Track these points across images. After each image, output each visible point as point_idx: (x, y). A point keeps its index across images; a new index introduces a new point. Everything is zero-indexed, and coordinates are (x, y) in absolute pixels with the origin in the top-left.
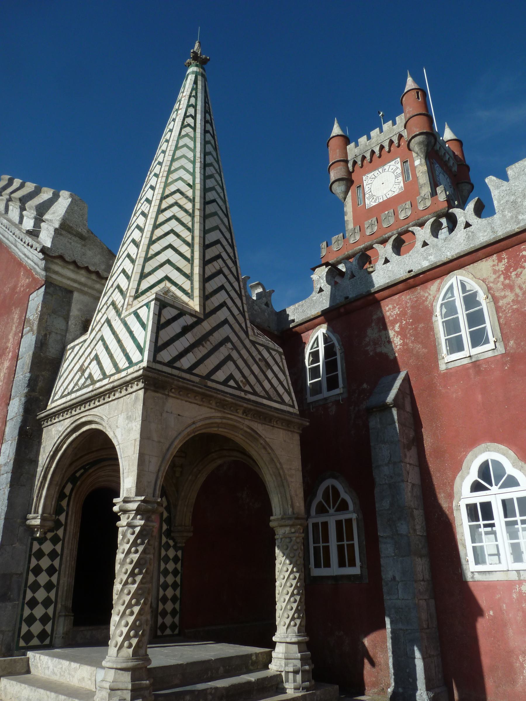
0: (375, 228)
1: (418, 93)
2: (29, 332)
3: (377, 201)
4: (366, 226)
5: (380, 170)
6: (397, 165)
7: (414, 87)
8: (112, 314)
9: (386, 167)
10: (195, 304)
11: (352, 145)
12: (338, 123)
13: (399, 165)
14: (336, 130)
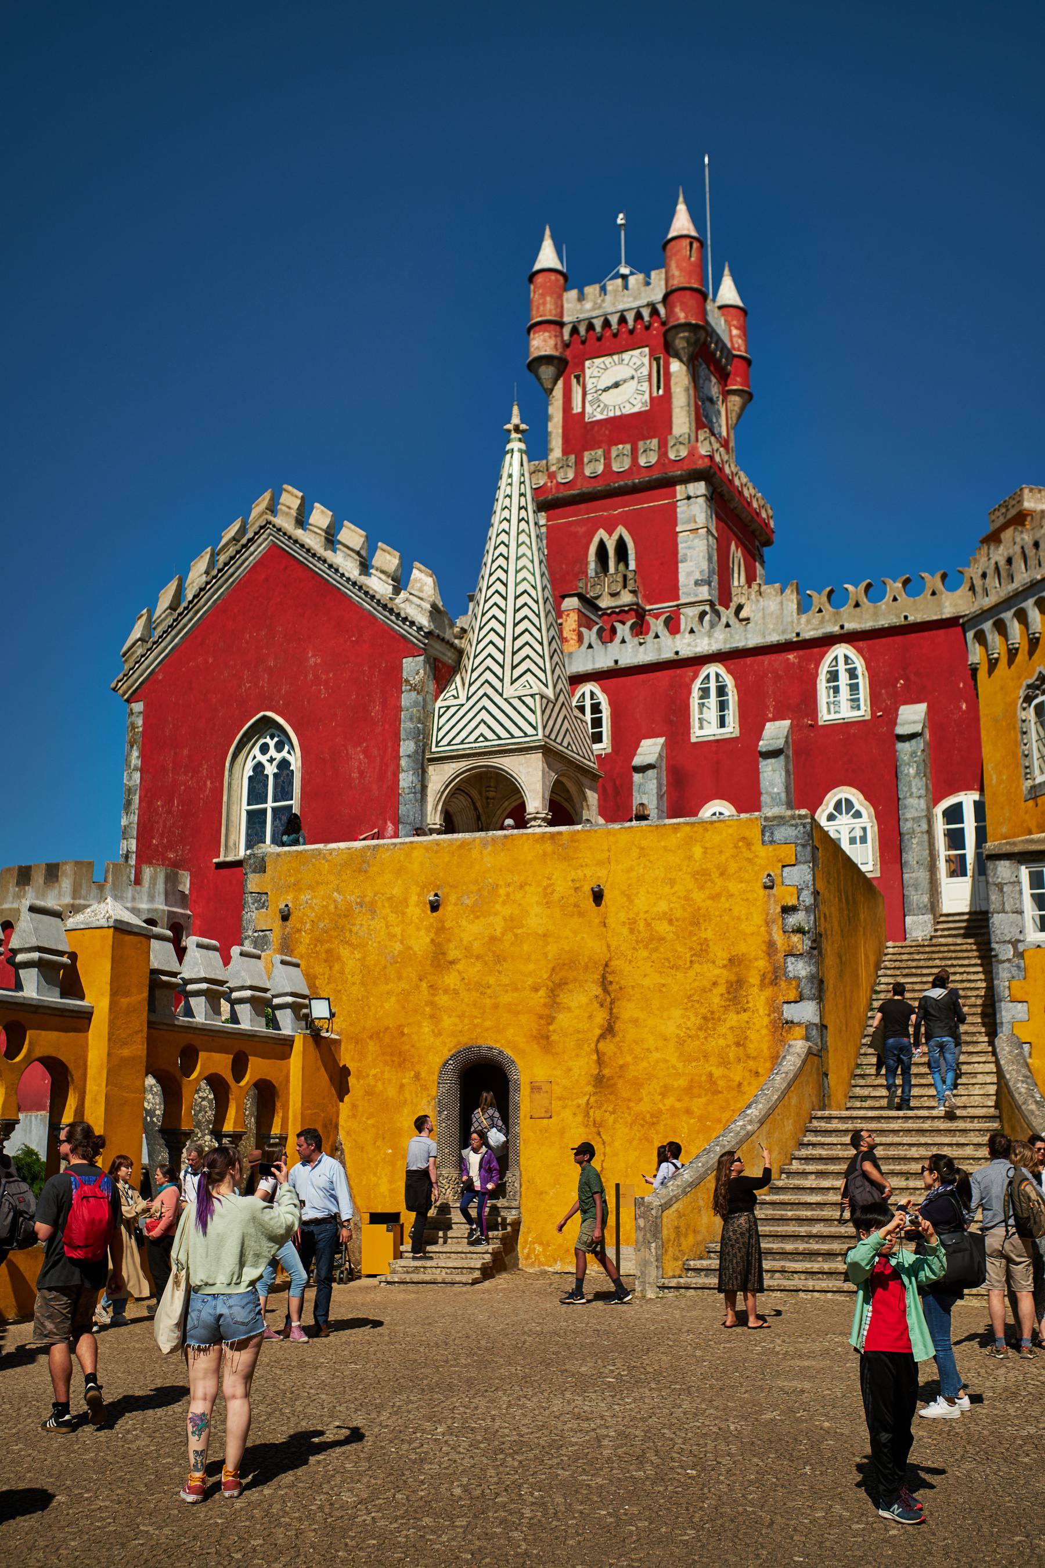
0: (600, 469)
1: (691, 244)
2: (410, 690)
3: (605, 413)
4: (586, 460)
5: (616, 357)
7: (685, 232)
8: (490, 692)
9: (626, 356)
10: (550, 693)
11: (573, 294)
12: (553, 237)
13: (646, 361)
14: (548, 257)
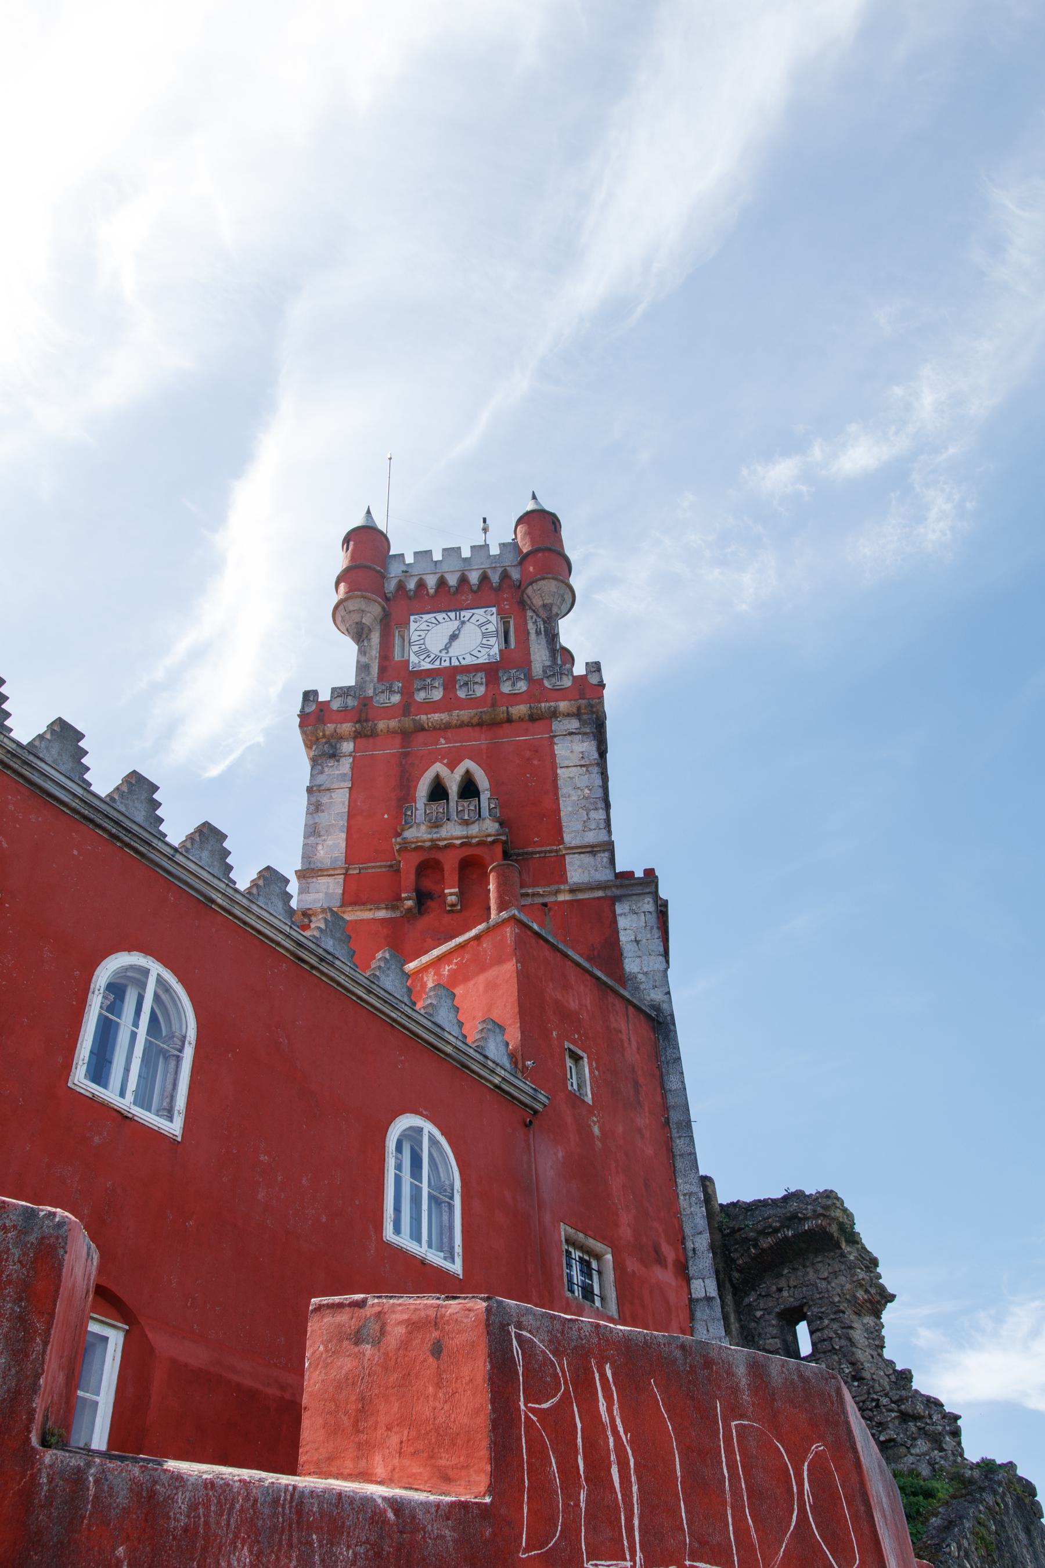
3: (437, 663)
5: (452, 615)
6: (489, 617)
13: (494, 619)
